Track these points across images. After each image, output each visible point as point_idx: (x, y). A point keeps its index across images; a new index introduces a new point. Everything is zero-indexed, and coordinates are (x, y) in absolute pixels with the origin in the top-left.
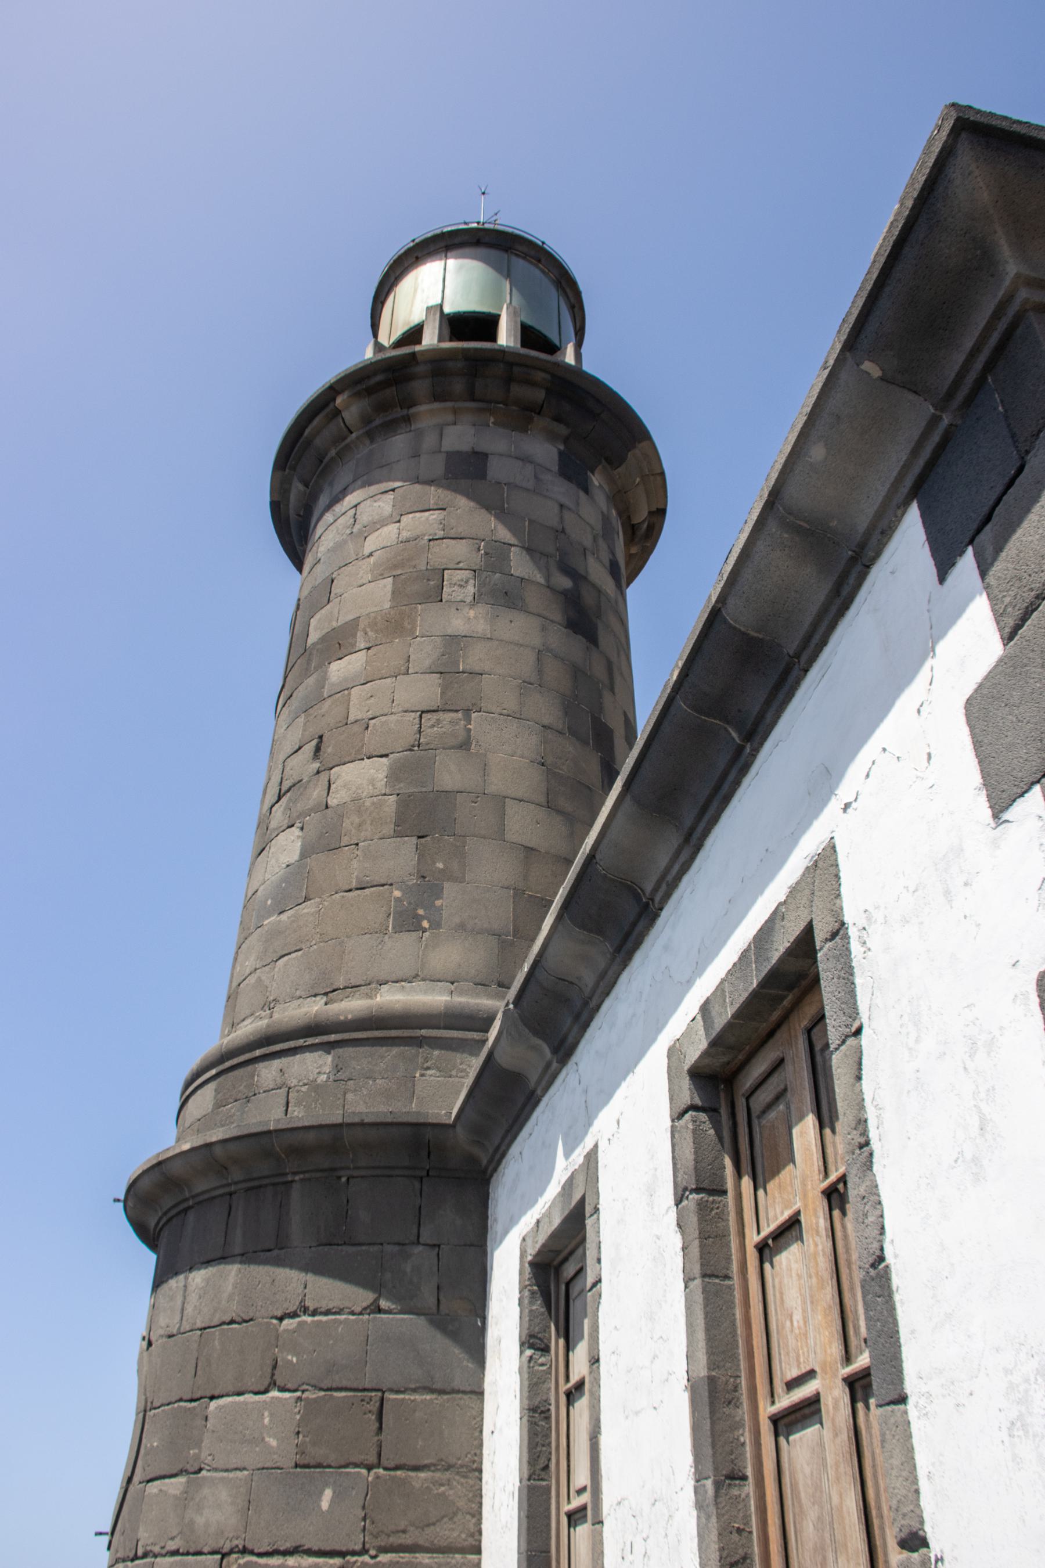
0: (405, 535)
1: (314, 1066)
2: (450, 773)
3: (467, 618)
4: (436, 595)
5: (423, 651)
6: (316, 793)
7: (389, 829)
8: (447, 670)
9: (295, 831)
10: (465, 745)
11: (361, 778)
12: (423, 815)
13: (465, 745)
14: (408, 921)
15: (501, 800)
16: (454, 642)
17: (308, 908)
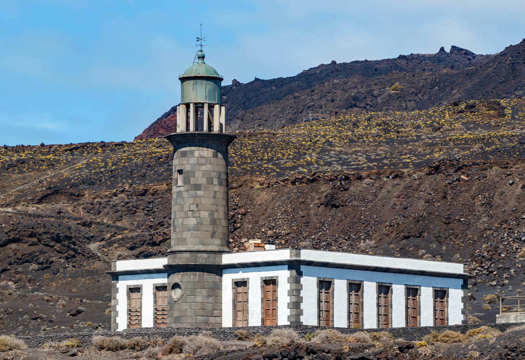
0: (207, 169)
1: (205, 255)
2: (216, 216)
3: (217, 188)
4: (212, 183)
5: (212, 195)
6: (197, 214)
7: (209, 223)
8: (214, 197)
9: (194, 219)
10: (217, 211)
11: (205, 214)
12: (213, 222)
13: (217, 211)
14: (212, 237)
15: (221, 219)
16: (215, 192)
17: (199, 232)
